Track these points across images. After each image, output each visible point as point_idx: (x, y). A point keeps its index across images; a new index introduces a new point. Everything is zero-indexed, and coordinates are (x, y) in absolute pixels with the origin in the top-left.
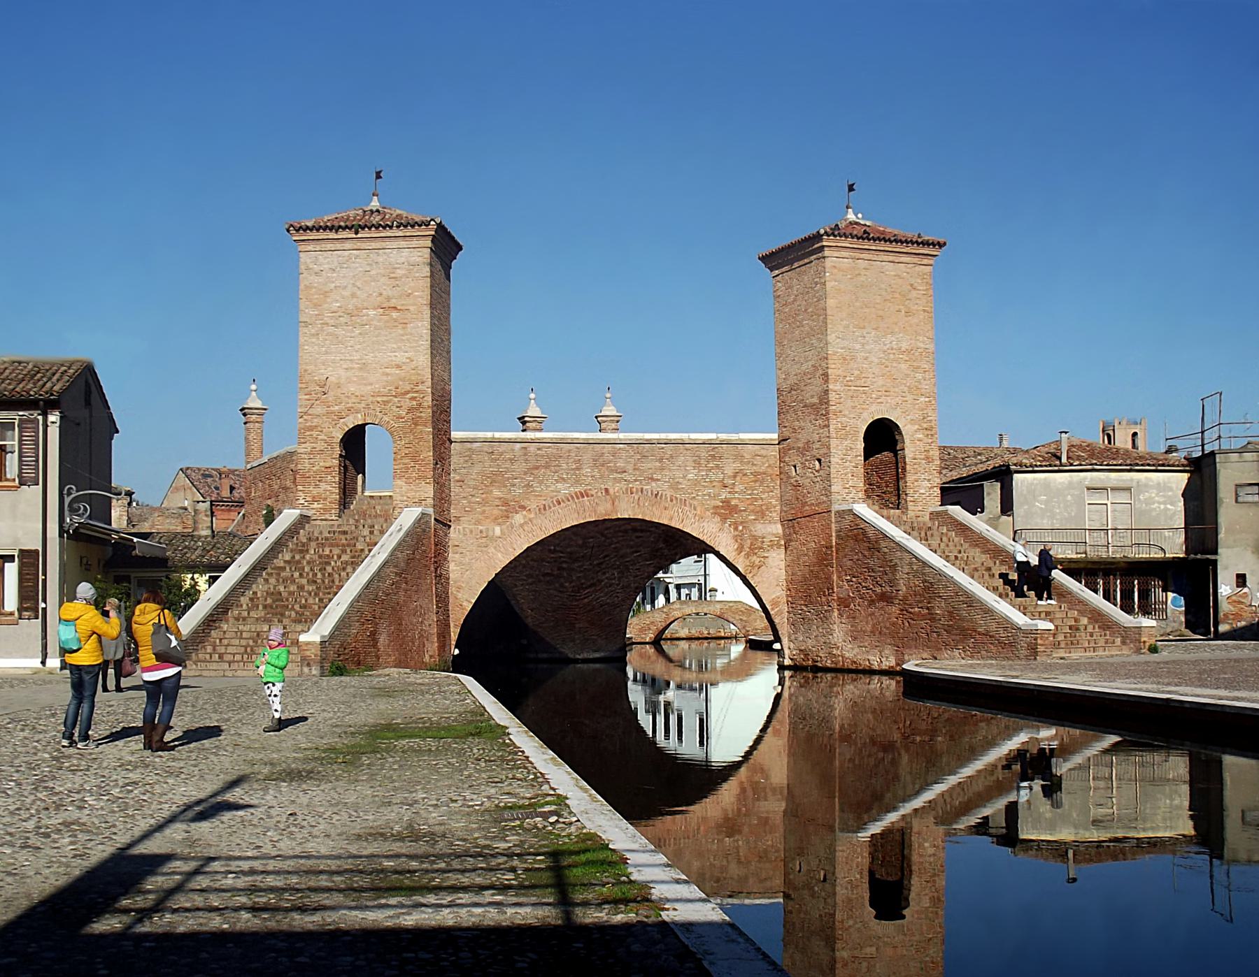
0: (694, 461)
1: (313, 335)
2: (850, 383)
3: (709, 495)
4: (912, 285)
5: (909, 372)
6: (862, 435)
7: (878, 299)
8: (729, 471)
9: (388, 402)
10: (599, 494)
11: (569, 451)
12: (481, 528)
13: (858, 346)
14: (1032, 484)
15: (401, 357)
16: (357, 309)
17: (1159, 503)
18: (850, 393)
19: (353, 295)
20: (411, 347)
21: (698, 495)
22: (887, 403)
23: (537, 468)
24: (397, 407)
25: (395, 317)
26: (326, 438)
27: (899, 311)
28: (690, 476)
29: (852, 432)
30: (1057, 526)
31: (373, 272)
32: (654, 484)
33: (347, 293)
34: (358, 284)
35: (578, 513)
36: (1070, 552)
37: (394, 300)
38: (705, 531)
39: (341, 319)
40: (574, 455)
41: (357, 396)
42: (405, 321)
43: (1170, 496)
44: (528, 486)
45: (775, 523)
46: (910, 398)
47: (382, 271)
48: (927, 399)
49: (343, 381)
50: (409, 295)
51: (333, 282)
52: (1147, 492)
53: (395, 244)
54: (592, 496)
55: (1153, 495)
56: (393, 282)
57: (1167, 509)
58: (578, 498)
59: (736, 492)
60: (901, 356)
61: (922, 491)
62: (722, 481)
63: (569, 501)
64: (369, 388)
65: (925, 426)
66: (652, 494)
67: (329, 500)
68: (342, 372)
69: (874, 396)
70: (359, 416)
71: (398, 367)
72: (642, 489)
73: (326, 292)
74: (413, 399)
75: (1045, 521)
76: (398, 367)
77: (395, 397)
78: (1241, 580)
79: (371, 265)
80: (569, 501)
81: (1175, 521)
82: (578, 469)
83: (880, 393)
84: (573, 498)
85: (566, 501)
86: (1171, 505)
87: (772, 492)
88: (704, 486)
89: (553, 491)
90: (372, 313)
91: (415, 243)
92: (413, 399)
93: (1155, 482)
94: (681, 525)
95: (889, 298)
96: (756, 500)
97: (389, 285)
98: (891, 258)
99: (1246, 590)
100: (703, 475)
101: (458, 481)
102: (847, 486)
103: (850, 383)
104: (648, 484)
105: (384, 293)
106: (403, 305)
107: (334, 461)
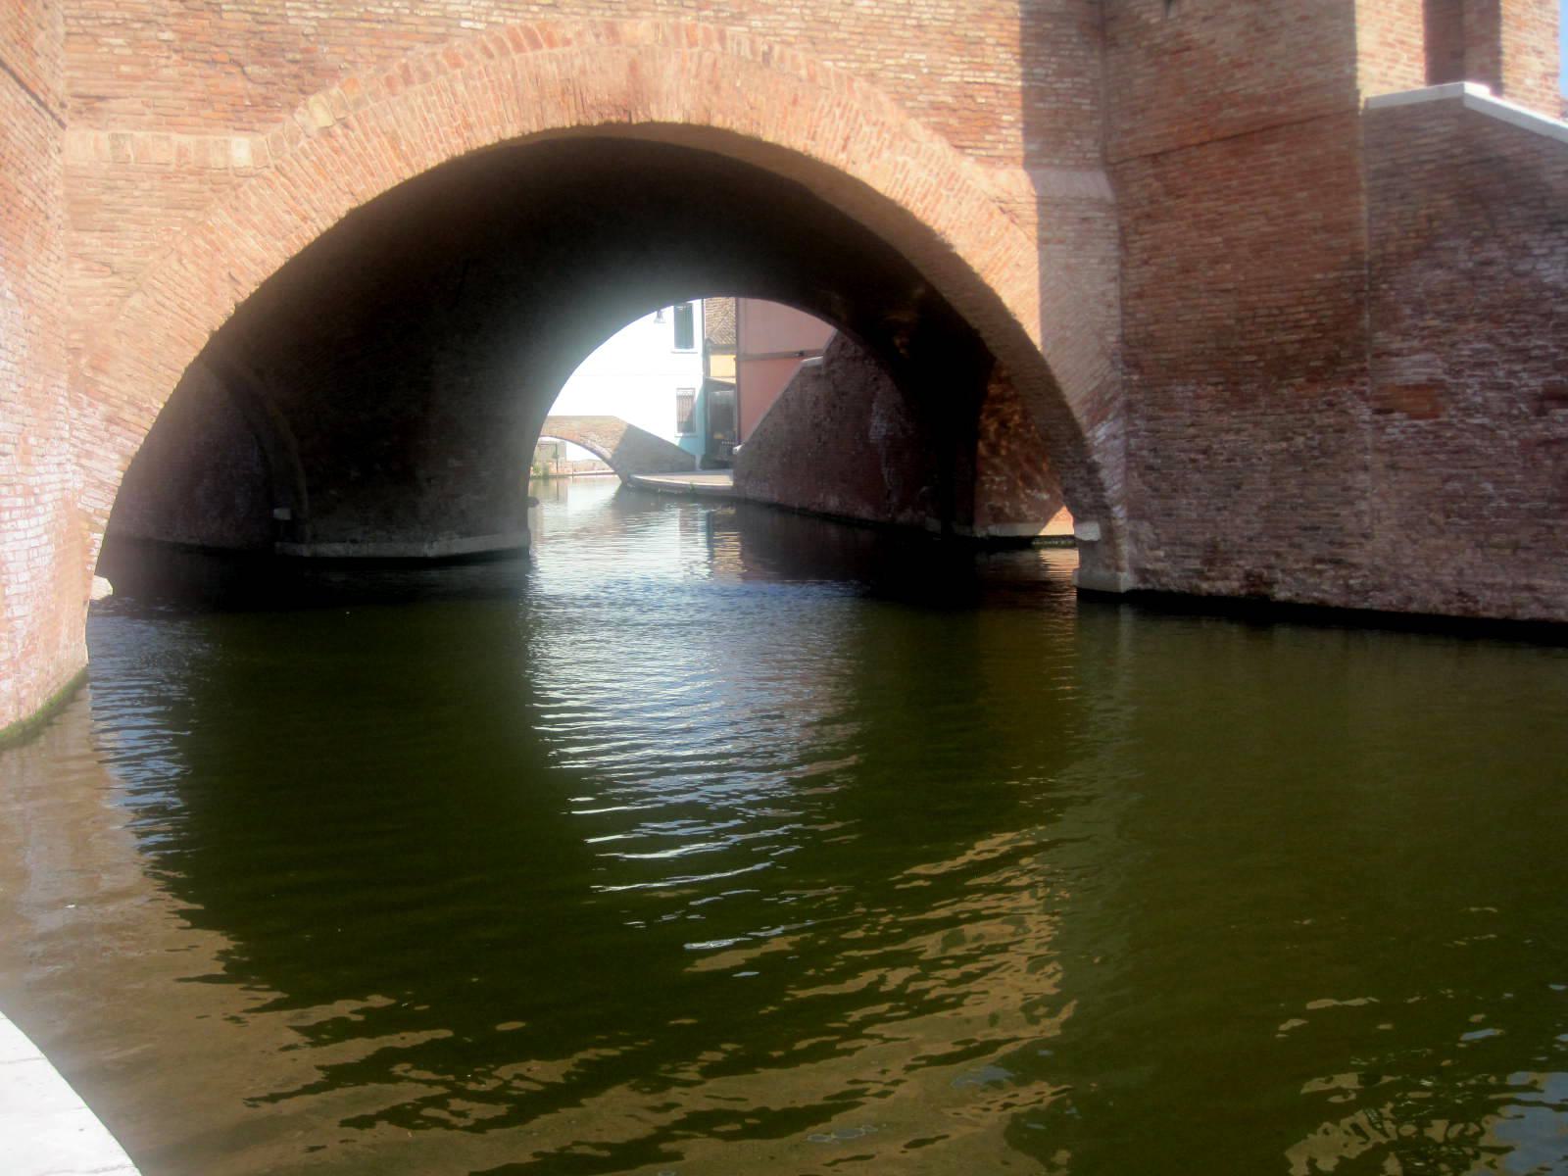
3: (913, 67)
10: (590, 39)
12: (178, 138)
21: (885, 68)
38: (911, 182)
54: (567, 42)
58: (519, 48)
59: (989, 67)
61: (1529, 82)
63: (491, 56)
66: (754, 52)
80: (491, 56)
85: (478, 55)
87: (1079, 74)
88: (902, 41)
89: (431, 22)
94: (842, 156)
102: (1391, 37)
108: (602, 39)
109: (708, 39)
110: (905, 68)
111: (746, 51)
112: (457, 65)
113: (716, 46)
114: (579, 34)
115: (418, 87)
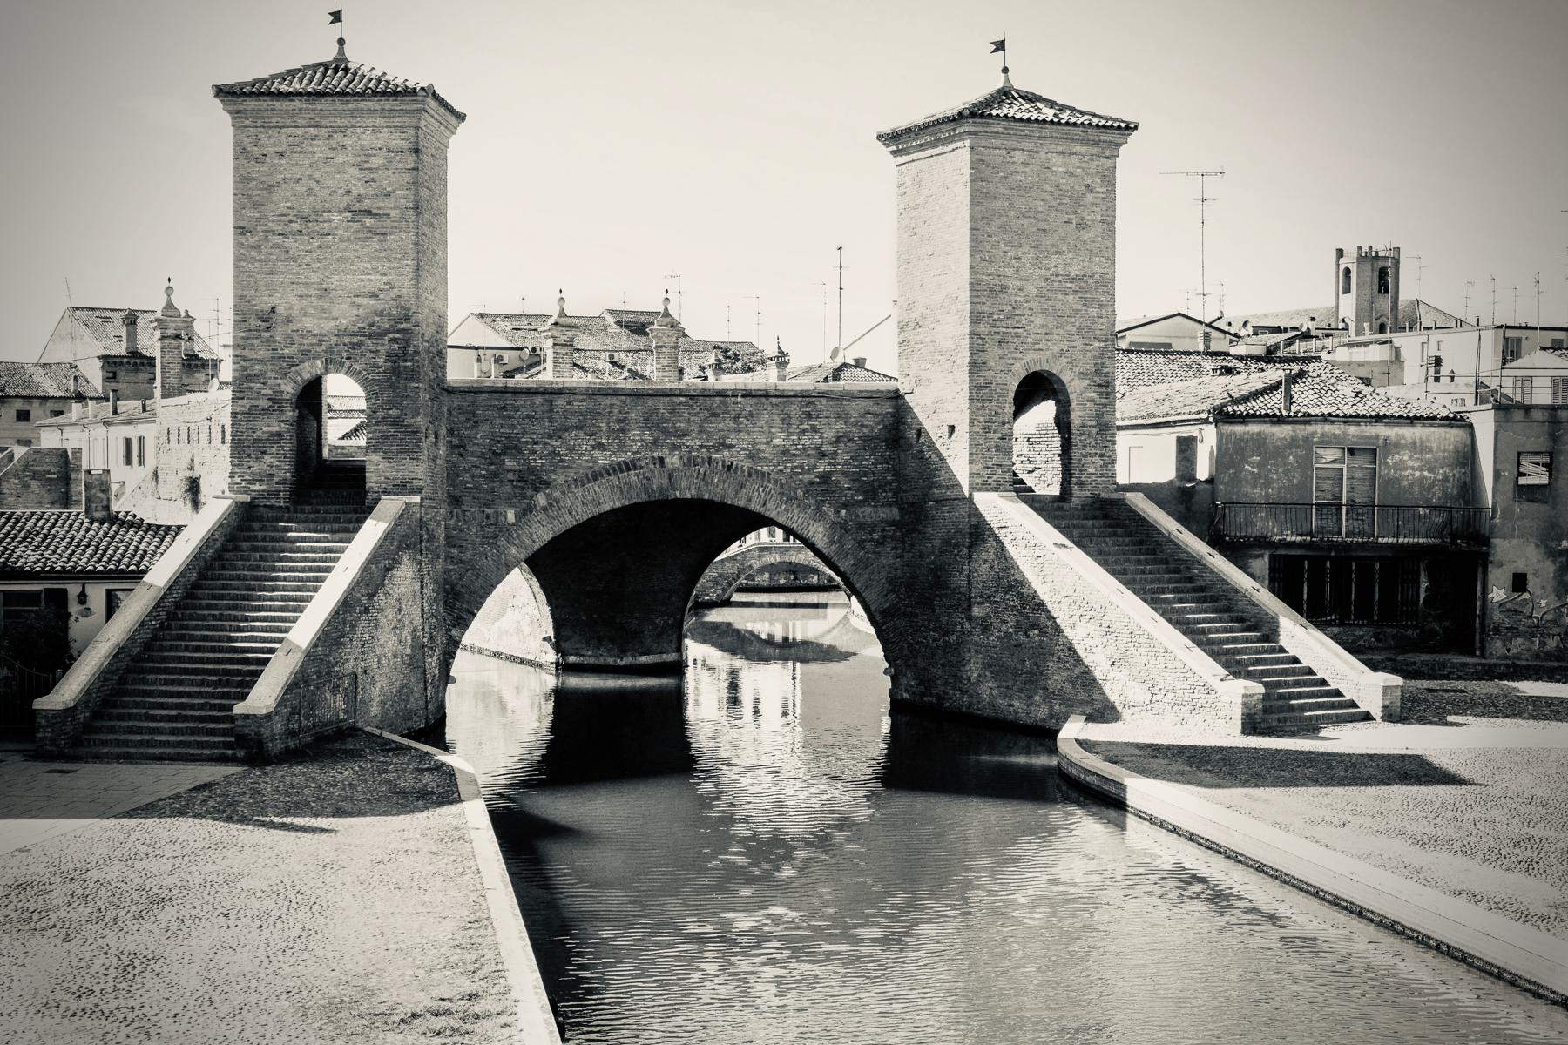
0: (783, 420)
1: (253, 247)
2: (998, 324)
3: (801, 467)
4: (1088, 186)
5: (1079, 307)
6: (1012, 395)
7: (1041, 206)
8: (830, 434)
9: (360, 344)
10: (651, 466)
11: (612, 405)
13: (1010, 272)
14: (1242, 440)
15: (377, 282)
16: (316, 212)
17: (1413, 468)
18: (998, 338)
19: (310, 192)
20: (390, 268)
22: (1048, 349)
23: (567, 429)
24: (371, 352)
25: (368, 224)
26: (270, 392)
27: (1069, 222)
28: (777, 441)
29: (998, 391)
30: (1274, 497)
31: (339, 160)
32: (726, 452)
33: (301, 188)
34: (317, 175)
35: (622, 492)
36: (1289, 532)
37: (367, 202)
39: (293, 224)
40: (616, 411)
41: (314, 335)
42: (383, 231)
43: (1427, 461)
44: (553, 454)
45: (890, 506)
46: (1079, 342)
47: (352, 160)
48: (1102, 344)
49: (295, 312)
50: (388, 194)
51: (281, 172)
52: (1398, 453)
53: (369, 122)
54: (642, 468)
55: (1406, 458)
56: (369, 176)
57: (1424, 477)
59: (839, 464)
60: (1069, 285)
61: (1092, 470)
62: (818, 448)
64: (332, 324)
65: (1097, 380)
66: (723, 466)
67: (276, 479)
68: (294, 301)
69: (1030, 340)
70: (318, 362)
71: (374, 296)
72: (710, 458)
73: (270, 186)
74: (394, 340)
75: (1257, 491)
76: (374, 296)
77: (370, 337)
78: (1519, 582)
79: (334, 149)
81: (1434, 493)
82: (623, 431)
83: (1038, 337)
84: (614, 471)
86: (1429, 472)
87: (888, 463)
88: (794, 455)
89: (587, 461)
90: (335, 217)
91: (397, 121)
92: (394, 340)
93: (1410, 441)
95: (1054, 203)
96: (865, 474)
97: (360, 179)
98: (1060, 149)
99: (1526, 596)
100: (793, 441)
101: (458, 446)
102: (990, 464)
103: (998, 324)
104: (717, 451)
105: (355, 192)
106: (379, 208)
107: (283, 425)
108: (657, 466)
109: (703, 462)
110: (796, 467)
111: (720, 466)
112: (596, 479)
113: (707, 465)
114: (647, 464)
115: (580, 489)
